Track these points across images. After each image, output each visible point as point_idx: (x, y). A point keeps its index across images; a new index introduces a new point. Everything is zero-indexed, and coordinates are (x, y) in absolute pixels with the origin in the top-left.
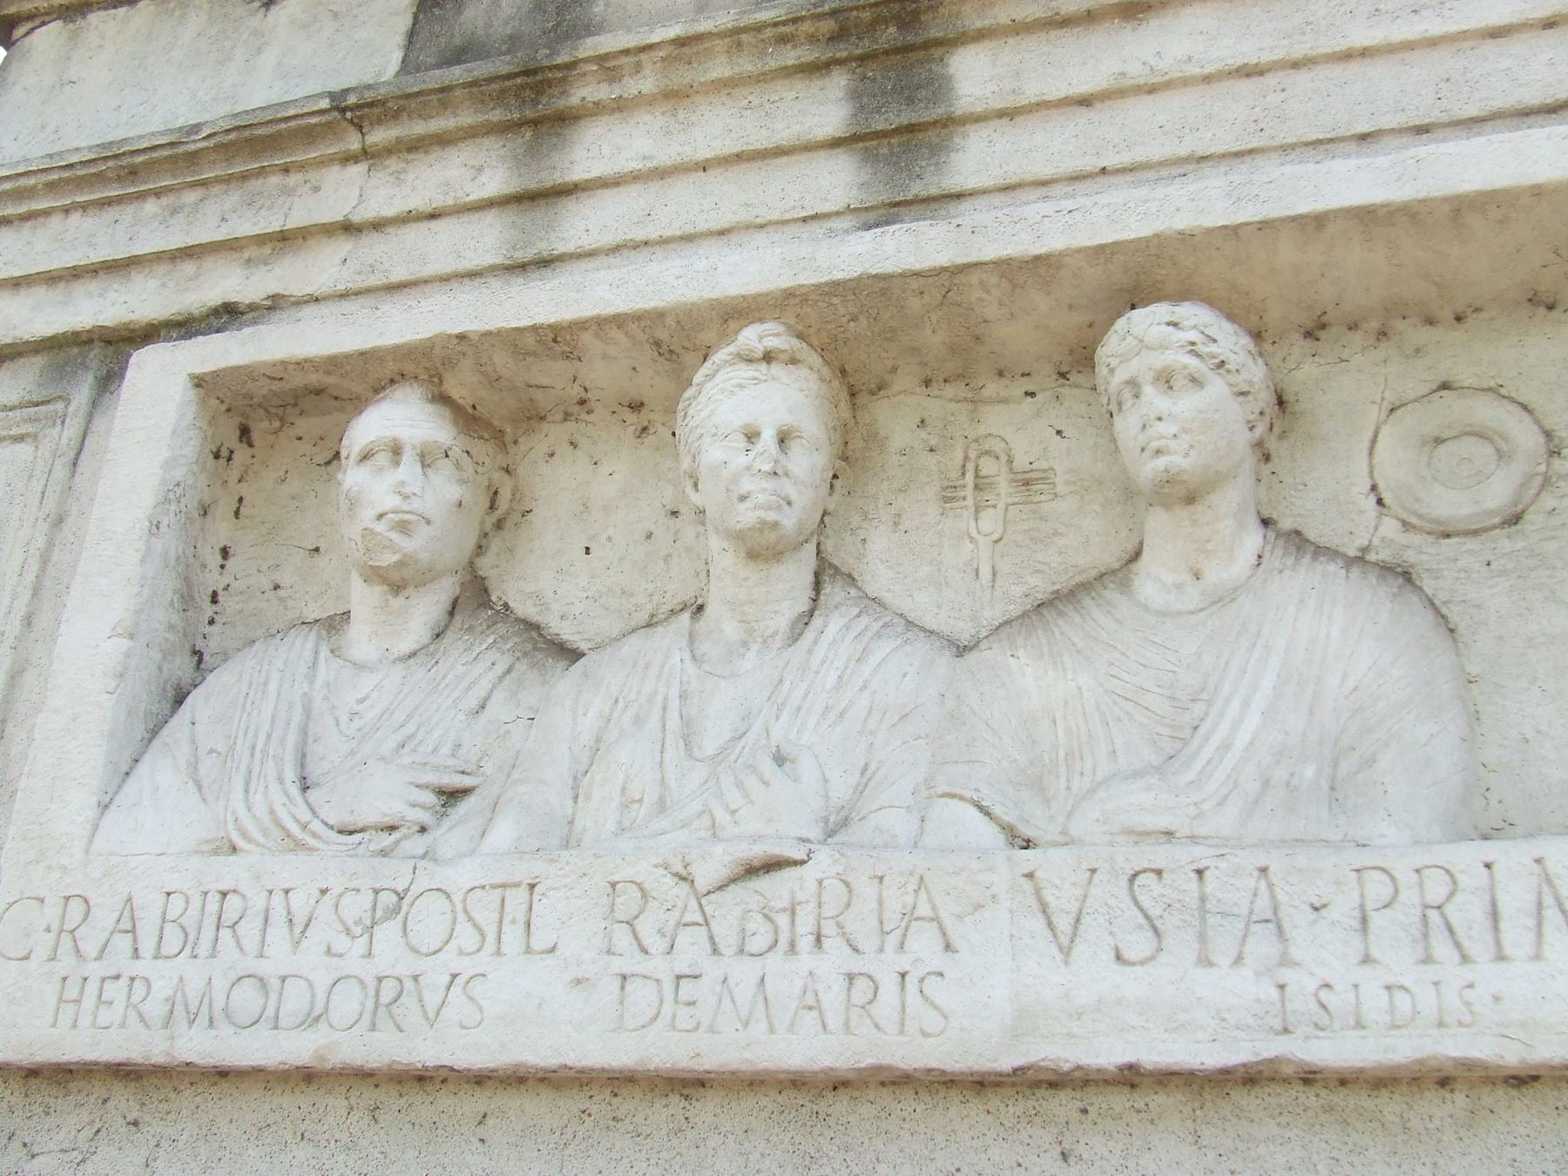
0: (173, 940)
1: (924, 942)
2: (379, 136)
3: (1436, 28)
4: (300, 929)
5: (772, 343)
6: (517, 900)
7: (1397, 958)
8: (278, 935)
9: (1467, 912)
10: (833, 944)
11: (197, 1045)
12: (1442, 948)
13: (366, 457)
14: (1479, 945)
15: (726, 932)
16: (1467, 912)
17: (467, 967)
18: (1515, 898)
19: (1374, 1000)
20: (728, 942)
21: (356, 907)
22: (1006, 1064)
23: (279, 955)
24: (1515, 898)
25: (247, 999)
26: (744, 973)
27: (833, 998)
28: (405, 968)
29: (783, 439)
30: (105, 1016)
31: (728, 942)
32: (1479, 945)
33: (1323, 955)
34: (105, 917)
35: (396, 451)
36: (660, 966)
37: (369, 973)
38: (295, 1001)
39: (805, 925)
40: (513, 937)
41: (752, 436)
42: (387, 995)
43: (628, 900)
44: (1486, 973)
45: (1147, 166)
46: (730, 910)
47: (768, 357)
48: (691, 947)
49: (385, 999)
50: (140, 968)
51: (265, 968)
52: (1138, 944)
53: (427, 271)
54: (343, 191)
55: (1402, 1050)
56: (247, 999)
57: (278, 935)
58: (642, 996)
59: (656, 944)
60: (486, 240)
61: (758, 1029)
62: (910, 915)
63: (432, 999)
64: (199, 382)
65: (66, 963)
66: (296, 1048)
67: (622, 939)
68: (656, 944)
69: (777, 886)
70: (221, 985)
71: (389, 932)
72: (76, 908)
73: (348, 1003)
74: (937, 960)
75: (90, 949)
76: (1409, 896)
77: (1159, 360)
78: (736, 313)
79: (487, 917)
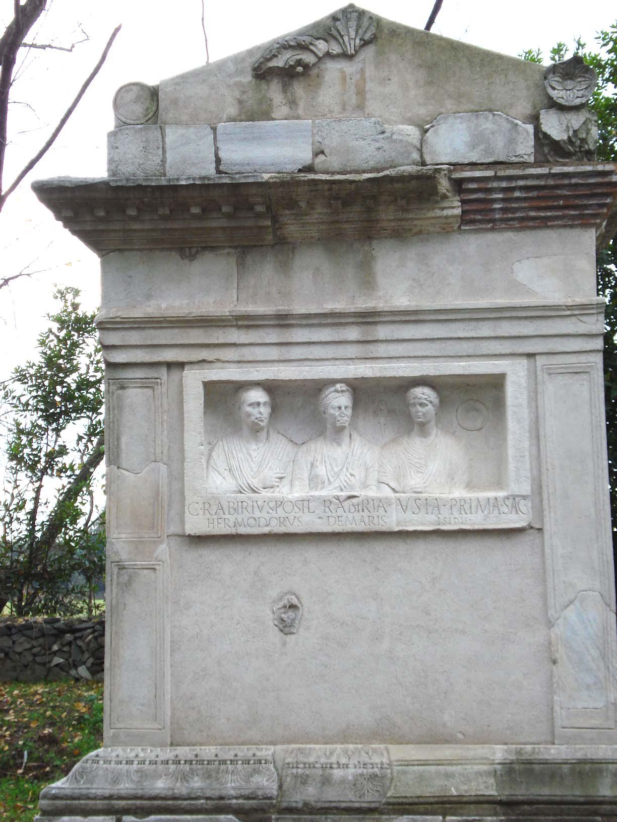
0: (232, 511)
1: (381, 511)
2: (240, 323)
3: (475, 336)
4: (261, 509)
5: (344, 389)
6: (306, 503)
7: (456, 514)
8: (256, 510)
9: (467, 506)
10: (366, 510)
11: (242, 530)
12: (463, 512)
13: (251, 405)
14: (468, 512)
15: (346, 509)
16: (467, 506)
17: (297, 515)
18: (474, 504)
19: (453, 521)
20: (347, 510)
21: (272, 504)
22: (397, 529)
23: (257, 514)
24: (474, 504)
25: (252, 521)
26: (350, 516)
27: (366, 520)
28: (285, 515)
29: (346, 408)
30: (220, 526)
31: (347, 510)
32: (468, 512)
33: (445, 512)
34: (214, 508)
35: (258, 404)
36: (335, 514)
37: (277, 516)
38: (263, 522)
39: (360, 508)
40: (306, 510)
41: (340, 408)
42: (282, 519)
43: (328, 503)
44: (469, 516)
45: (418, 357)
46: (346, 504)
47: (342, 391)
48: (340, 511)
49: (282, 521)
50: (227, 516)
51: (254, 516)
52: (417, 511)
53: (258, 359)
54: (234, 336)
55: (456, 527)
56: (252, 521)
57: (256, 510)
58: (332, 520)
59: (334, 511)
60: (274, 353)
61: (354, 525)
62: (379, 506)
63: (291, 521)
64: (203, 382)
65: (208, 516)
66: (266, 530)
67: (327, 509)
68: (334, 511)
69: (354, 501)
70: (245, 520)
71: (280, 510)
72: (207, 506)
73: (274, 522)
74: (384, 513)
75: (213, 512)
76: (458, 504)
77: (420, 401)
78: (334, 382)
79: (300, 507)
